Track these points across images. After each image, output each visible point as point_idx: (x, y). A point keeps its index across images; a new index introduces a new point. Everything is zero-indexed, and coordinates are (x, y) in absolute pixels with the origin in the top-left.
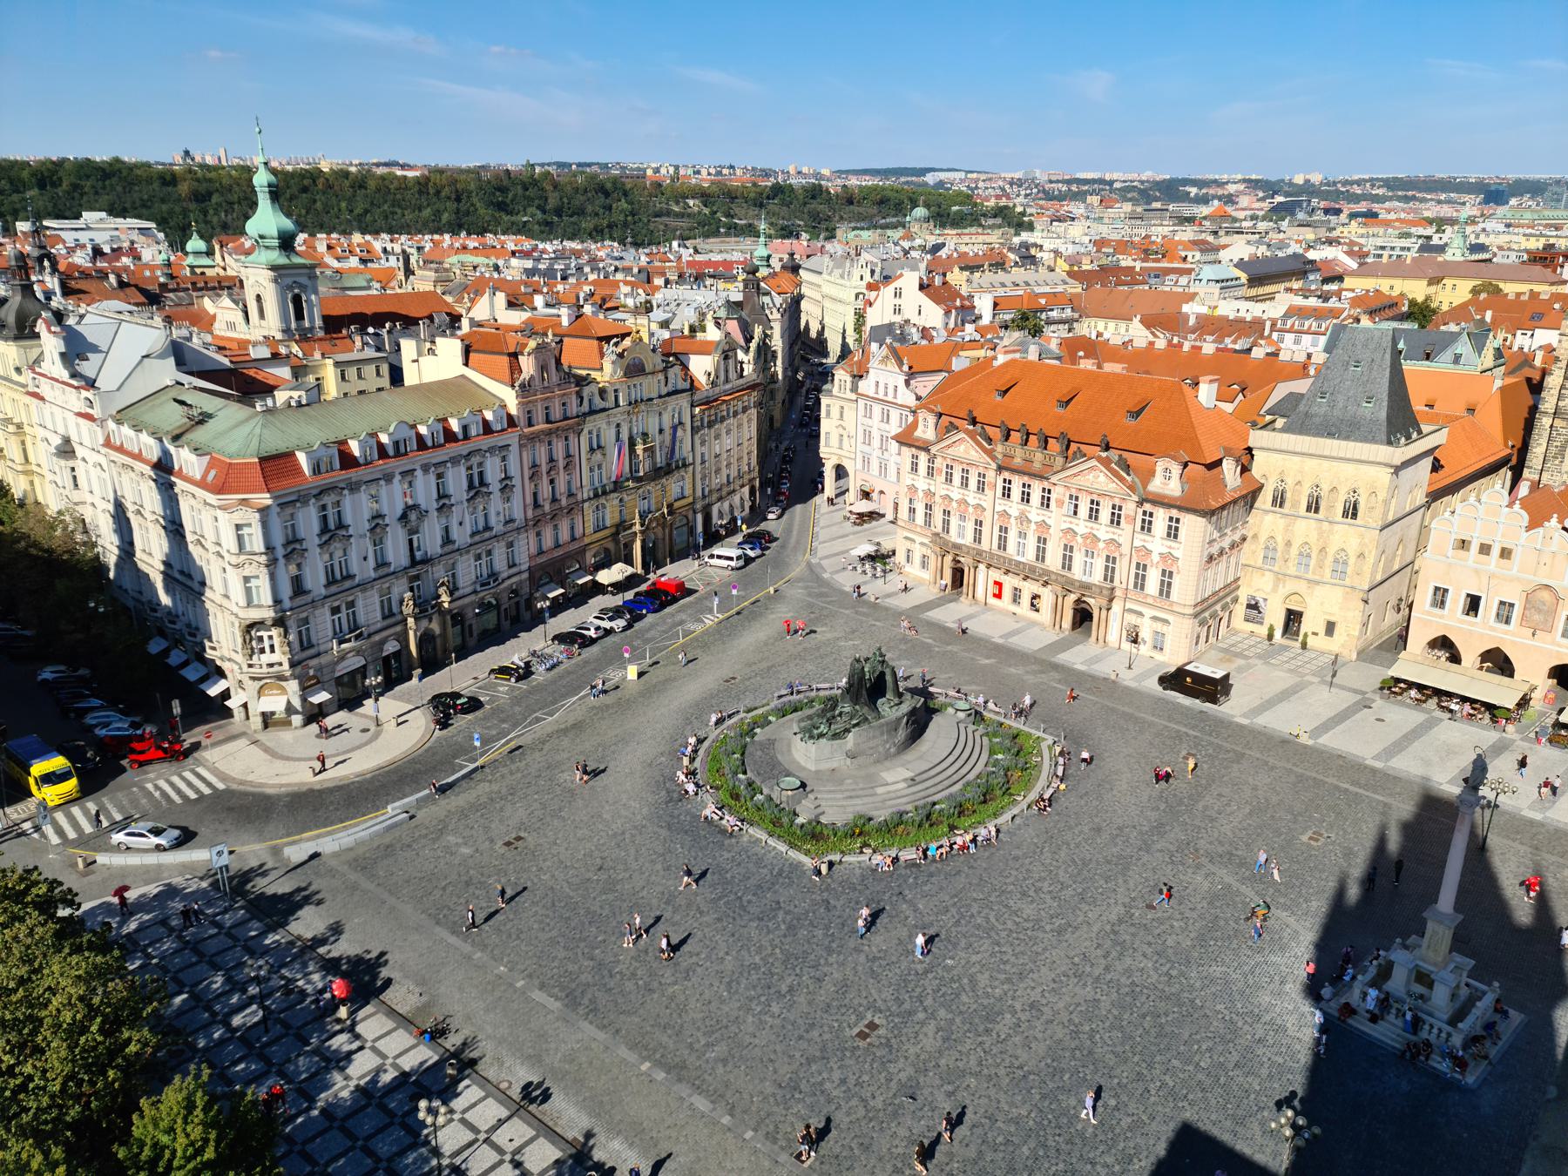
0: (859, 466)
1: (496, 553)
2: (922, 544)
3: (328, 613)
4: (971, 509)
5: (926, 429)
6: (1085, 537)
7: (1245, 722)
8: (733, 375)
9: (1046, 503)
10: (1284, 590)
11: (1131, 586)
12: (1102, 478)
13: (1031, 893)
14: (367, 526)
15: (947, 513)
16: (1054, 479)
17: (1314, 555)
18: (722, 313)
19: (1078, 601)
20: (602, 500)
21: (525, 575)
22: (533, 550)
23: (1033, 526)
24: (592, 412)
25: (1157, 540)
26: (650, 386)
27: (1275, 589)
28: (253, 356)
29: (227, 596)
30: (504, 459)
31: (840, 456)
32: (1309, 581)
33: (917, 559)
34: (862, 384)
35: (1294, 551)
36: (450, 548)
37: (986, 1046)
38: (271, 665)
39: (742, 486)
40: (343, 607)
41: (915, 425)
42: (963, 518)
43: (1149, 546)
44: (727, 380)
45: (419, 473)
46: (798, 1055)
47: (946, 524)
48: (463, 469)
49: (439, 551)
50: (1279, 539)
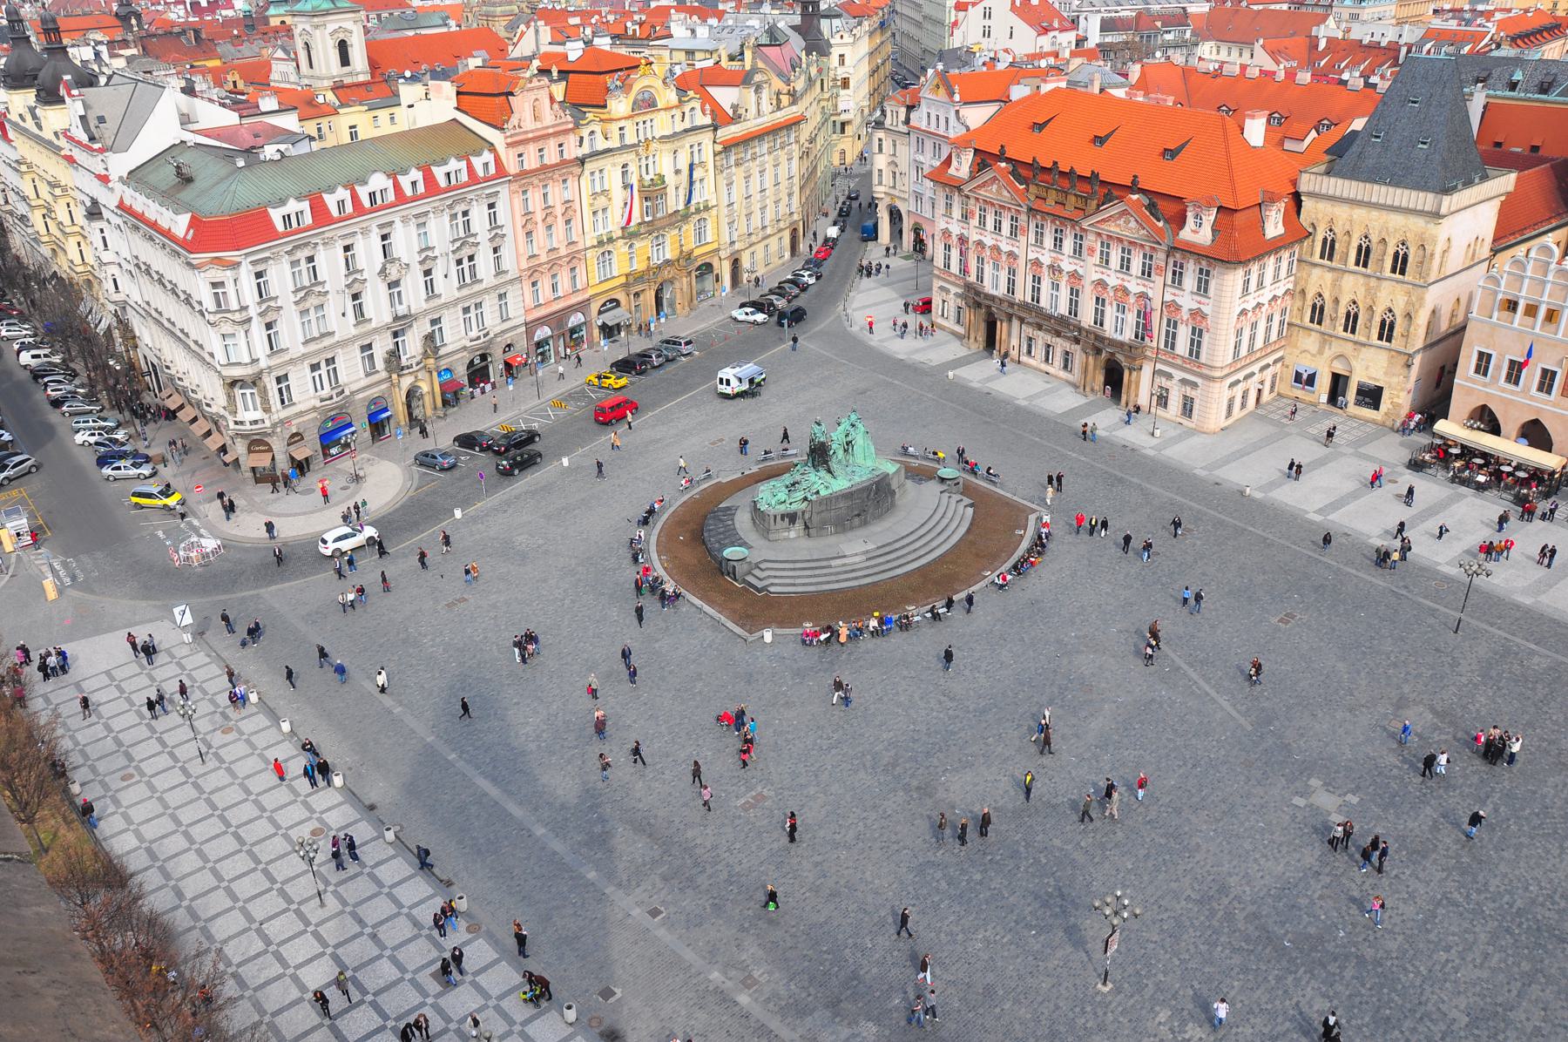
1: (486, 308)
3: (308, 370)
5: (962, 167)
6: (1116, 290)
7: (1258, 495)
8: (766, 106)
9: (1078, 251)
10: (1328, 353)
11: (1162, 346)
12: (1133, 224)
13: (967, 672)
14: (344, 282)
15: (980, 260)
16: (1085, 225)
18: (765, 40)
19: (1108, 361)
22: (530, 302)
23: (1066, 278)
26: (662, 124)
27: (1321, 352)
28: (263, 109)
29: (212, 355)
30: (491, 206)
31: (893, 197)
32: (1356, 343)
35: (1342, 312)
36: (436, 302)
37: (869, 822)
38: (256, 422)
39: (780, 230)
40: (323, 364)
41: (948, 162)
42: (996, 267)
46: (677, 820)
47: (980, 272)
48: (447, 218)
49: (425, 306)
50: (1326, 295)
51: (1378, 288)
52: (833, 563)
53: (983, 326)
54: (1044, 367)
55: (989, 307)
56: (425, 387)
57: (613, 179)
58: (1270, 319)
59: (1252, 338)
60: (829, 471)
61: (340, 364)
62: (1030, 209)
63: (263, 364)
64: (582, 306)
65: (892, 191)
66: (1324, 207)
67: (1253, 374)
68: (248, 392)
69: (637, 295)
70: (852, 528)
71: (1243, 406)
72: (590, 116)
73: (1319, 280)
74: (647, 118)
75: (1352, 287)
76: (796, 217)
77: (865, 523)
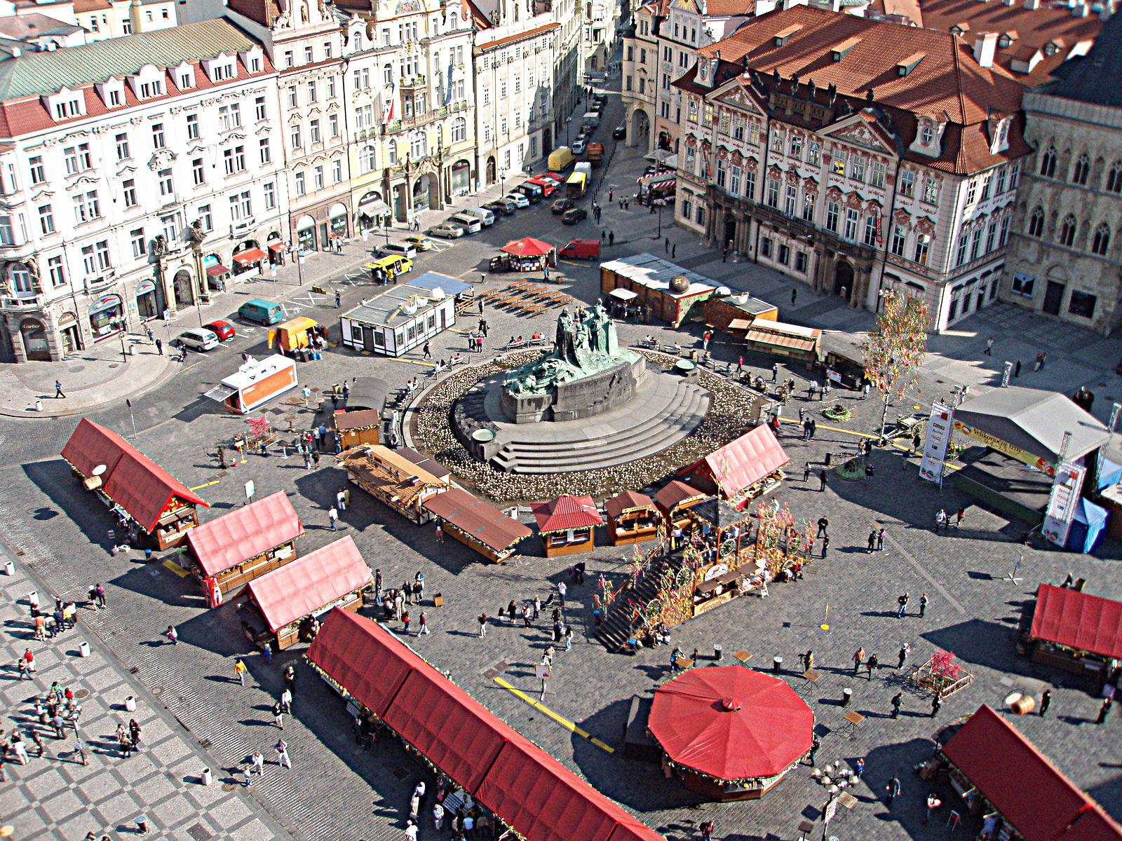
0: (659, 112)
2: (699, 196)
4: (744, 162)
8: (524, 13)
11: (891, 249)
12: (867, 136)
16: (821, 133)
17: (1078, 228)
19: (839, 263)
20: (370, 142)
21: (285, 219)
23: (802, 183)
24: (362, 53)
25: (916, 202)
31: (642, 102)
32: (1072, 254)
33: (694, 214)
34: (662, 26)
35: (1059, 223)
36: (203, 190)
37: (605, 692)
39: (536, 130)
41: (694, 72)
43: (908, 208)
44: (517, 18)
45: (167, 115)
47: (722, 175)
50: (1046, 208)
51: (1095, 204)
52: (576, 446)
53: (722, 227)
54: (780, 267)
55: (728, 209)
56: (192, 272)
57: (377, 78)
58: (992, 228)
59: (975, 246)
60: (575, 362)
61: (111, 248)
62: (770, 118)
63: (38, 245)
64: (344, 199)
65: (641, 96)
66: (1047, 122)
67: (974, 280)
68: (21, 273)
69: (397, 188)
70: (594, 414)
71: (965, 309)
72: (356, 17)
73: (1040, 193)
74: (407, 20)
75: (1071, 201)
76: (548, 119)
77: (607, 410)
